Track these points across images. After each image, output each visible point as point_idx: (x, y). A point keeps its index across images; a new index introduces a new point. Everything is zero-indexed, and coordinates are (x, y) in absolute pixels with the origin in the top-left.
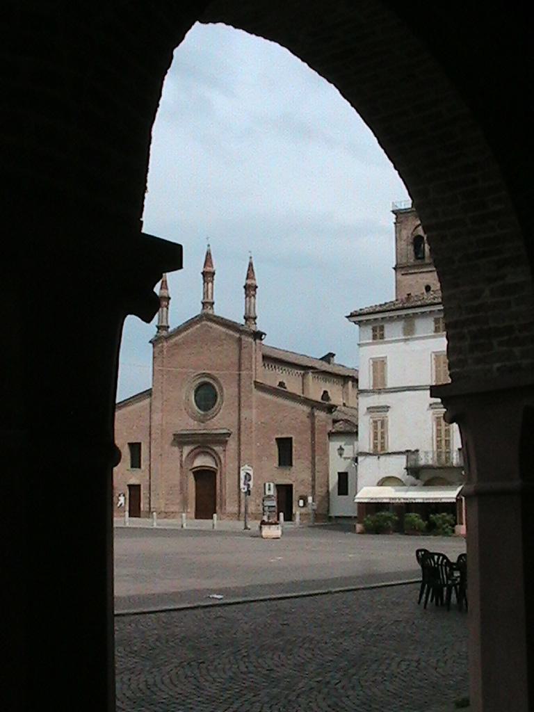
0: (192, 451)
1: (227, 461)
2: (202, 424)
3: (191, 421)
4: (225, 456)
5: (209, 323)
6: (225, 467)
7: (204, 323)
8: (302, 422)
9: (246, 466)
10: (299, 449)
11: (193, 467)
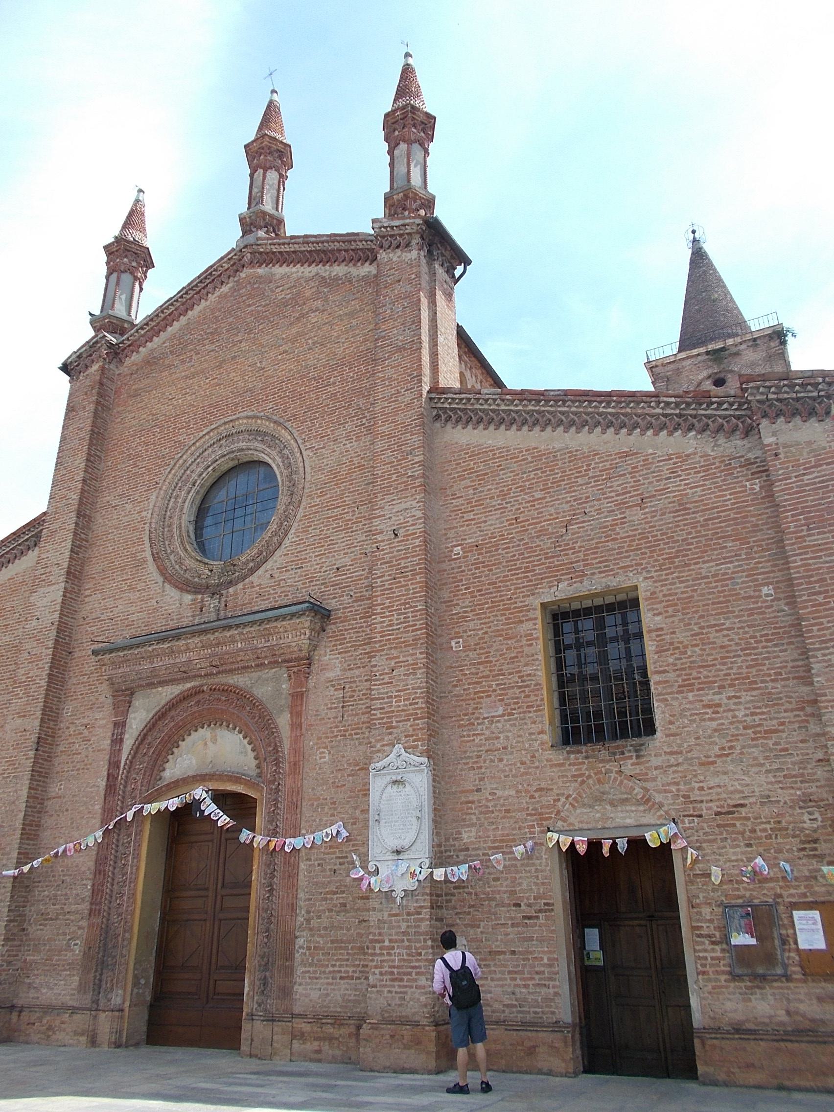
0: (161, 716)
2: (211, 603)
3: (172, 593)
4: (296, 725)
5: (261, 271)
6: (295, 765)
8: (682, 507)
9: (398, 748)
10: (681, 636)
11: (161, 784)
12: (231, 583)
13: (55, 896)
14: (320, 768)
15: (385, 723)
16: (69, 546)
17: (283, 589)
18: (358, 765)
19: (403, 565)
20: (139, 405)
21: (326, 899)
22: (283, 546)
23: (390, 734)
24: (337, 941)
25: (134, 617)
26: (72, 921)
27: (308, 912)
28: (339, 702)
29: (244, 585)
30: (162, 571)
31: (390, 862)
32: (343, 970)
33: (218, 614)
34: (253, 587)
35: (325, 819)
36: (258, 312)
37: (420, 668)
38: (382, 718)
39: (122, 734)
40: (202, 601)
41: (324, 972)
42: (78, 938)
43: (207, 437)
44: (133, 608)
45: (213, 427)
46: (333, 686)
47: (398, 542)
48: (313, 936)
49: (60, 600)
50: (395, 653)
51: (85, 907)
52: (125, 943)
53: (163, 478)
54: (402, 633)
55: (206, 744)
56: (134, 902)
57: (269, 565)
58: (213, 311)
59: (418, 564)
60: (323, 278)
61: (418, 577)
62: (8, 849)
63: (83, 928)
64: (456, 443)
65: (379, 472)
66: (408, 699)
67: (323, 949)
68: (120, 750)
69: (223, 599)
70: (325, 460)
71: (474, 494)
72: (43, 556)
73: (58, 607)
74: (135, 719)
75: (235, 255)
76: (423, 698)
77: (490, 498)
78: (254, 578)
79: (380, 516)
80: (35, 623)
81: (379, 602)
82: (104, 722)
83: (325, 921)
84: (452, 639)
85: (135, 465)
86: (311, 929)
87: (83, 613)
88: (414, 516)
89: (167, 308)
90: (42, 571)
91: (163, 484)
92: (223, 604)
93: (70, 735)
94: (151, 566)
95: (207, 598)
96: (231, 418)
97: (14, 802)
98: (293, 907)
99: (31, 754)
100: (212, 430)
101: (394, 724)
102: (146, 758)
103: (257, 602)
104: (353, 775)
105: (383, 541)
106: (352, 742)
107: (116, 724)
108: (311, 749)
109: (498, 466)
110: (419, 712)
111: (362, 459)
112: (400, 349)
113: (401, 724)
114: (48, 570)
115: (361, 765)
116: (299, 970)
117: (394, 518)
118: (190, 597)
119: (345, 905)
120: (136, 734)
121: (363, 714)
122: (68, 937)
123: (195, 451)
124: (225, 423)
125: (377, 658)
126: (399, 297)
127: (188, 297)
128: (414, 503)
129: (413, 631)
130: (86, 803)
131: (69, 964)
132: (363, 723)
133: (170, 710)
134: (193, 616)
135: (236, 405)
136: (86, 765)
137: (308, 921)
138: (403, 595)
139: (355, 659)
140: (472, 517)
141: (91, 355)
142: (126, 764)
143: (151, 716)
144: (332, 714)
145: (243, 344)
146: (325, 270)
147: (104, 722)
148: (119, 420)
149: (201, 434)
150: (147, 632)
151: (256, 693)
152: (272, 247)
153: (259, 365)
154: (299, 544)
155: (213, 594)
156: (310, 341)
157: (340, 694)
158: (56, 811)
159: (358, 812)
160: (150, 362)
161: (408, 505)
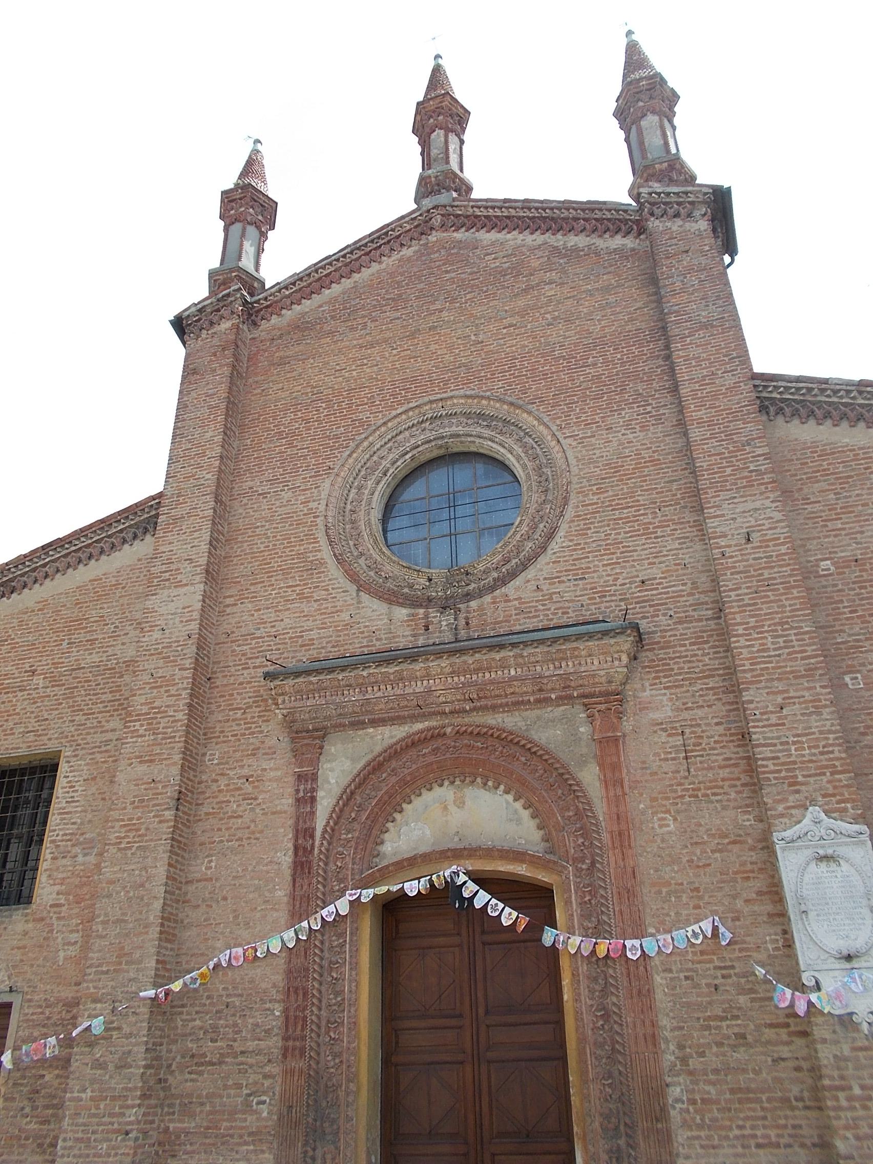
0: (375, 767)
1: (639, 804)
2: (443, 622)
5: (459, 235)
7: (433, 238)
9: (815, 811)
12: (468, 597)
13: (215, 1028)
14: (663, 841)
15: (785, 778)
16: (207, 537)
17: (558, 605)
18: (726, 836)
19: (766, 576)
20: (289, 375)
21: (708, 1028)
22: (549, 551)
23: (798, 792)
24: (740, 1090)
25: (314, 634)
26: (251, 1066)
27: (681, 1047)
28: (677, 752)
29: (494, 598)
30: (353, 577)
31: (837, 973)
32: (759, 1133)
33: (456, 634)
34: (509, 601)
35: (685, 912)
36: (463, 280)
37: (825, 706)
38: (779, 771)
39: (313, 790)
40: (426, 616)
41: (727, 1138)
42: (264, 1093)
43: (404, 417)
44: (310, 623)
45: (411, 405)
46: (662, 729)
47: (753, 548)
48: (695, 1082)
49: (199, 605)
50: (781, 686)
51: (274, 1043)
52: (350, 1099)
53: (340, 463)
54: (784, 660)
55: (445, 808)
56: (357, 1036)
57: (530, 573)
58: (392, 275)
59: (790, 576)
60: (556, 248)
61: (795, 591)
62: (137, 955)
63: (273, 1077)
64: (796, 440)
65: (705, 464)
66: (817, 747)
67: (717, 1102)
68: (313, 813)
69: (462, 616)
70: (597, 452)
71: (837, 499)
72: (162, 549)
73: (196, 615)
74: (332, 770)
75: (421, 215)
76: (839, 745)
77: (863, 505)
78: (510, 589)
79: (717, 516)
80: (157, 635)
81: (739, 620)
82: (279, 773)
83: (713, 1059)
84: (845, 673)
85: (291, 445)
86: (691, 1073)
87: (225, 627)
88: (772, 518)
89: (323, 268)
90: (164, 568)
91: (340, 469)
92: (462, 622)
93: (220, 791)
94: (334, 570)
95: (433, 613)
96: (439, 396)
97: (142, 885)
98: (653, 1040)
99: (169, 814)
100: (411, 409)
101: (800, 779)
102: (356, 826)
103: (518, 620)
104: (720, 851)
105: (729, 546)
106: (711, 806)
107: (300, 777)
108: (643, 813)
109: (866, 469)
110: (837, 763)
111: (654, 452)
112: (705, 326)
113: (812, 780)
114: (173, 567)
115: (733, 838)
116: (681, 1136)
117: (739, 520)
118: (405, 611)
119: (743, 1036)
120: (337, 791)
121: (720, 767)
122: (245, 1092)
123: (386, 432)
124: (431, 402)
125: (752, 692)
126: (690, 270)
127: (354, 257)
128: (767, 503)
129: (803, 659)
130: (258, 888)
131: (251, 1134)
132: (723, 780)
133: (390, 758)
134: (414, 636)
135: (446, 382)
136: (253, 833)
137: (684, 1060)
138: (777, 613)
139: (693, 696)
140: (840, 526)
141: (218, 310)
142: (325, 831)
143: (359, 765)
144: (669, 766)
145: (445, 314)
146: (558, 240)
147: (279, 773)
148: (259, 391)
149: (394, 413)
150: (337, 654)
151: (536, 737)
152: (475, 209)
153: (473, 338)
154: (575, 550)
155: (444, 608)
156: (548, 316)
157: (679, 741)
158: (204, 900)
159: (739, 904)
160: (301, 327)
161: (758, 504)
